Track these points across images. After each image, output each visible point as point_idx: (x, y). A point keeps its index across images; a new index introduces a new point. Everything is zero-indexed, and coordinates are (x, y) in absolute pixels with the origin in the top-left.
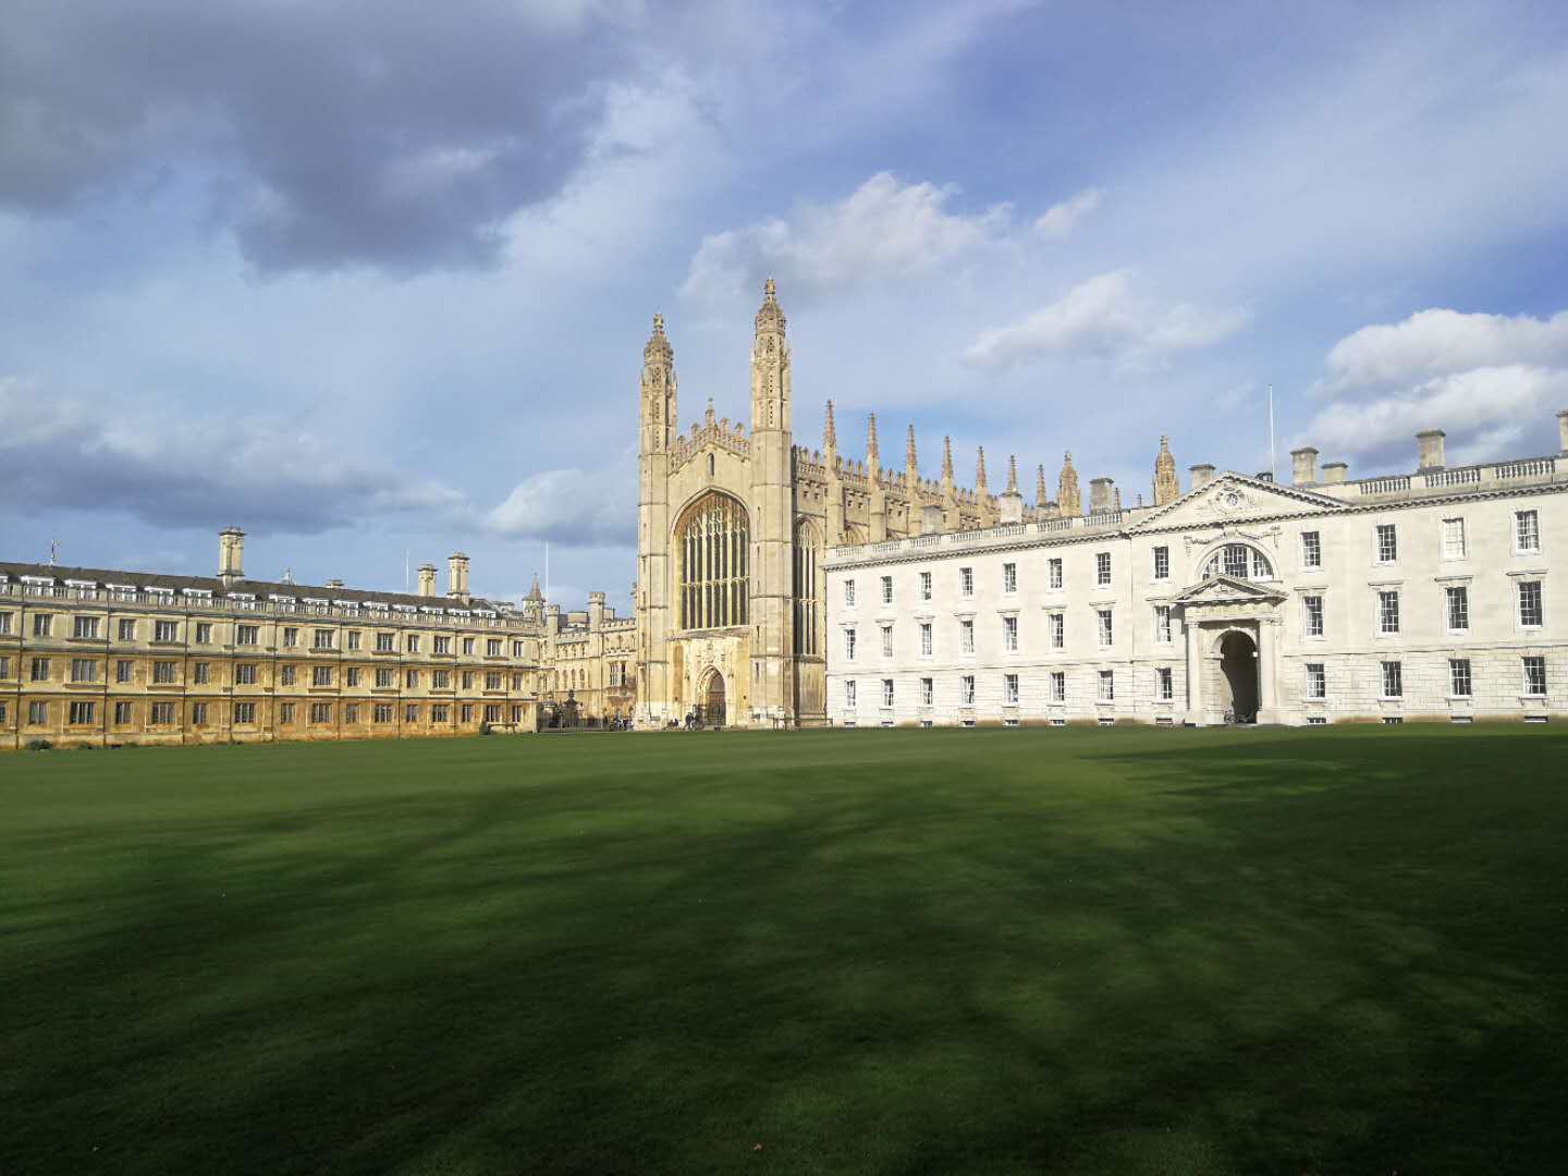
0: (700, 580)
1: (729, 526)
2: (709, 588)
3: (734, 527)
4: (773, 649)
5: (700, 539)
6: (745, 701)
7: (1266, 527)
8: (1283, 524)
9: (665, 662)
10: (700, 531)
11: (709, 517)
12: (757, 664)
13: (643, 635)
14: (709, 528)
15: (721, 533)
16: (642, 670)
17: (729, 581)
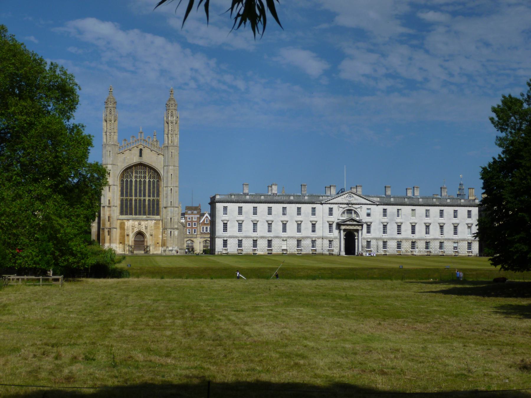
0: (131, 196)
1: (147, 178)
2: (136, 200)
3: (150, 178)
4: (176, 226)
5: (131, 181)
6: (158, 245)
7: (359, 206)
8: (363, 206)
9: (116, 228)
10: (131, 177)
11: (136, 172)
12: (171, 232)
13: (109, 217)
14: (136, 177)
15: (142, 180)
16: (109, 231)
17: (147, 198)
